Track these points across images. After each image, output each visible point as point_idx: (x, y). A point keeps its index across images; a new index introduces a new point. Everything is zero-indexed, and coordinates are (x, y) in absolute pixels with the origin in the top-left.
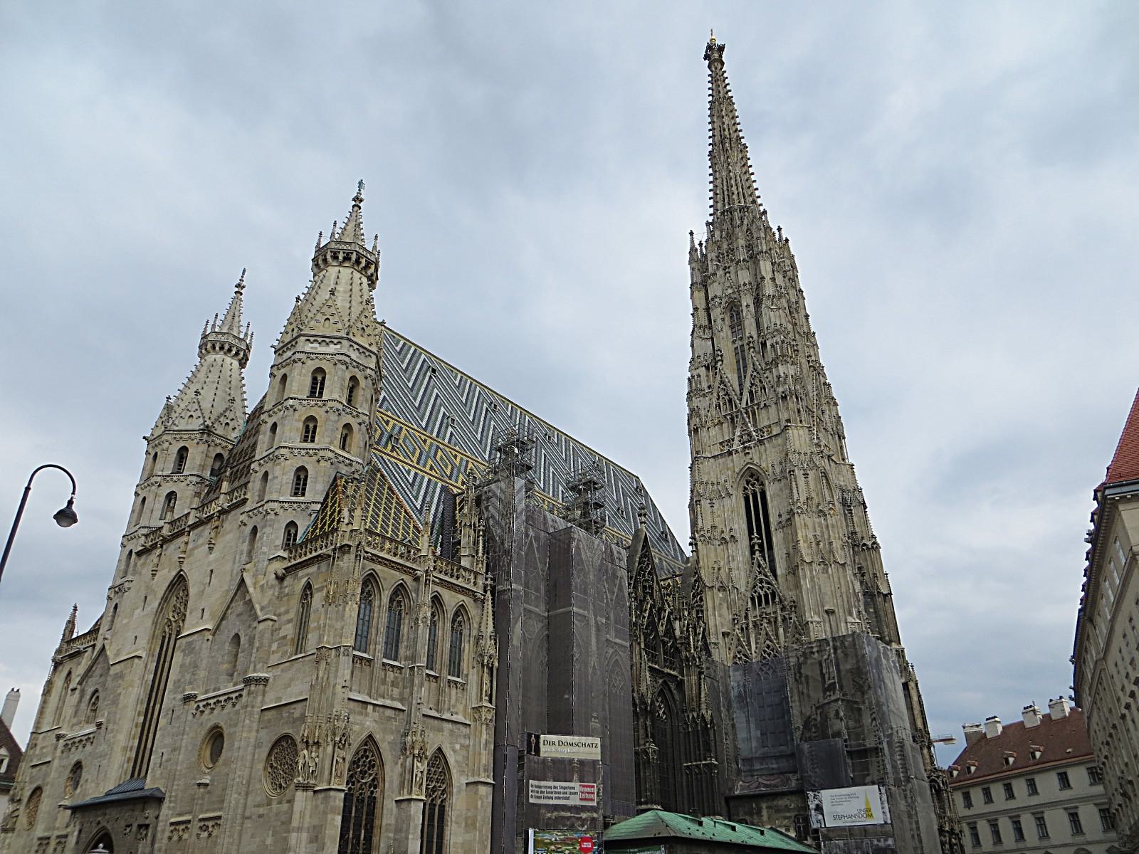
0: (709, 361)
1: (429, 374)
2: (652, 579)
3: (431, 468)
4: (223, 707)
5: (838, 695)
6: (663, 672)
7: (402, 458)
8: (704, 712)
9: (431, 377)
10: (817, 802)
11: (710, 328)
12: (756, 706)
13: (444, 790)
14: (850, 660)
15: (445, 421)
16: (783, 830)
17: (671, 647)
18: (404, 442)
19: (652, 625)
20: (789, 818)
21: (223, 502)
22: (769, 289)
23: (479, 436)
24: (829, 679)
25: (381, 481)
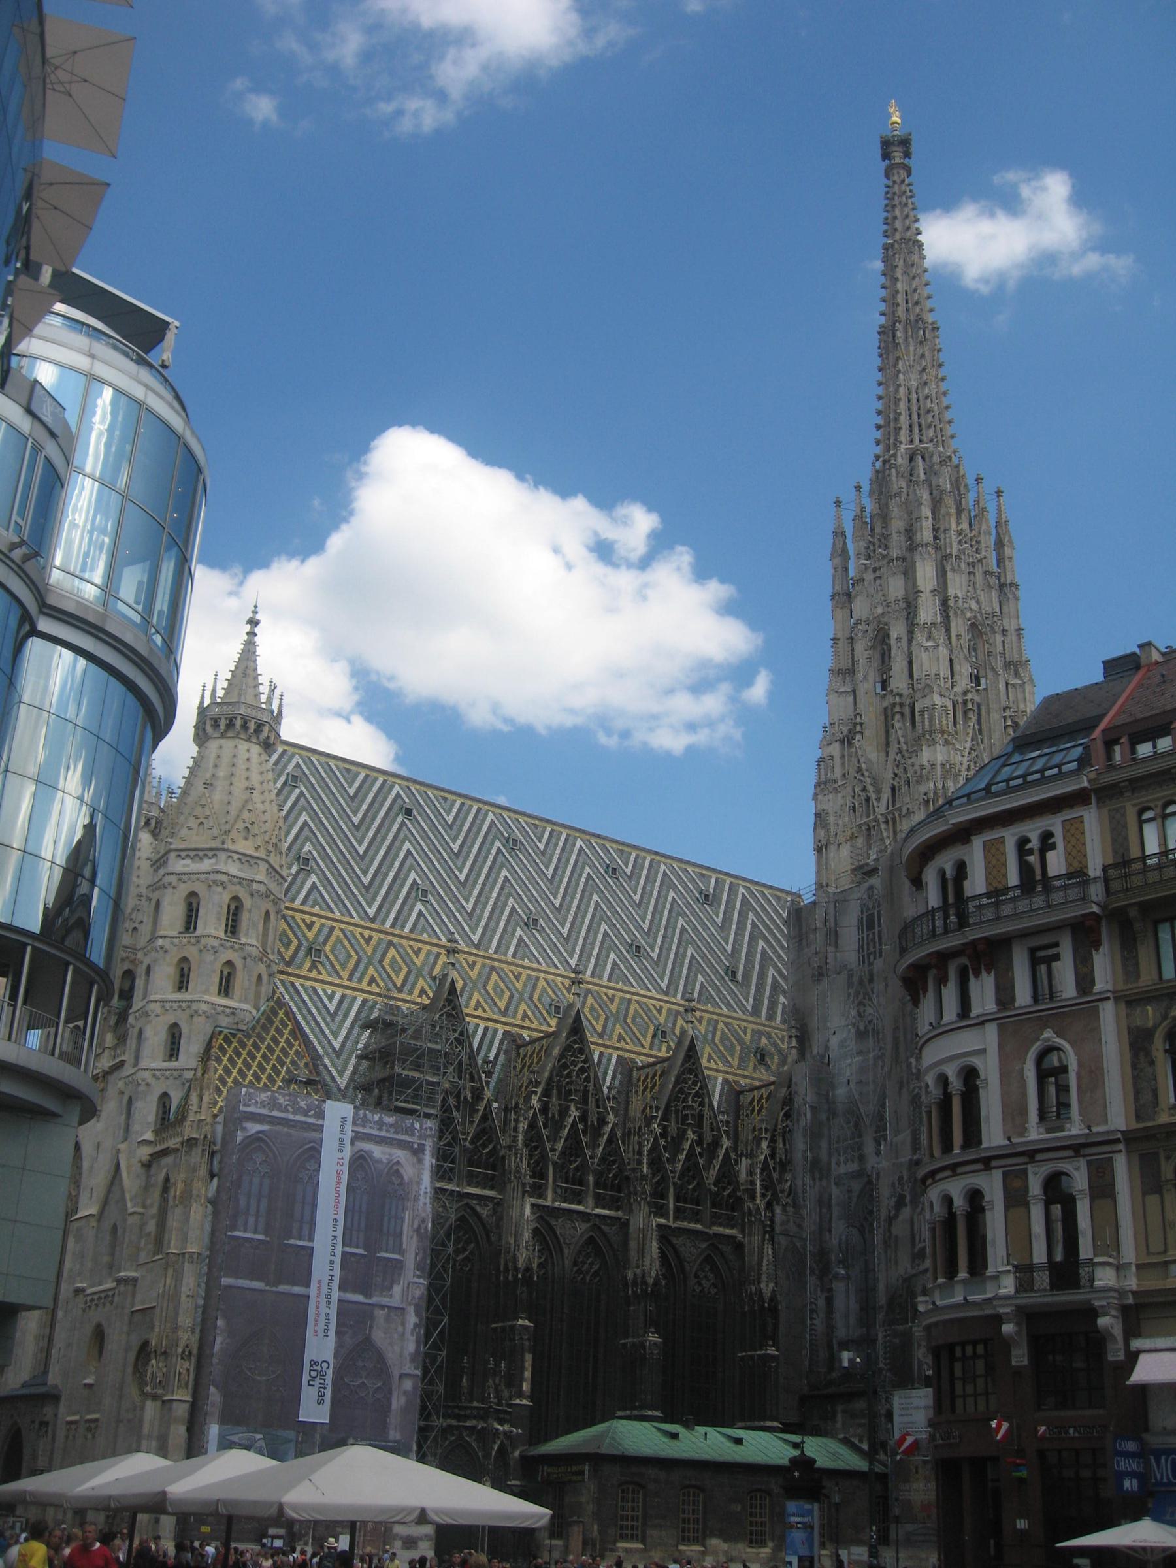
0: (845, 733)
1: (399, 819)
2: (702, 1104)
3: (372, 981)
4: (104, 1304)
5: (928, 1263)
6: (706, 1233)
7: (325, 977)
8: (763, 1286)
9: (403, 824)
11: (854, 672)
15: (413, 895)
16: (856, 1441)
17: (729, 1196)
19: (692, 1170)
21: (105, 1063)
23: (469, 907)
25: (282, 1021)
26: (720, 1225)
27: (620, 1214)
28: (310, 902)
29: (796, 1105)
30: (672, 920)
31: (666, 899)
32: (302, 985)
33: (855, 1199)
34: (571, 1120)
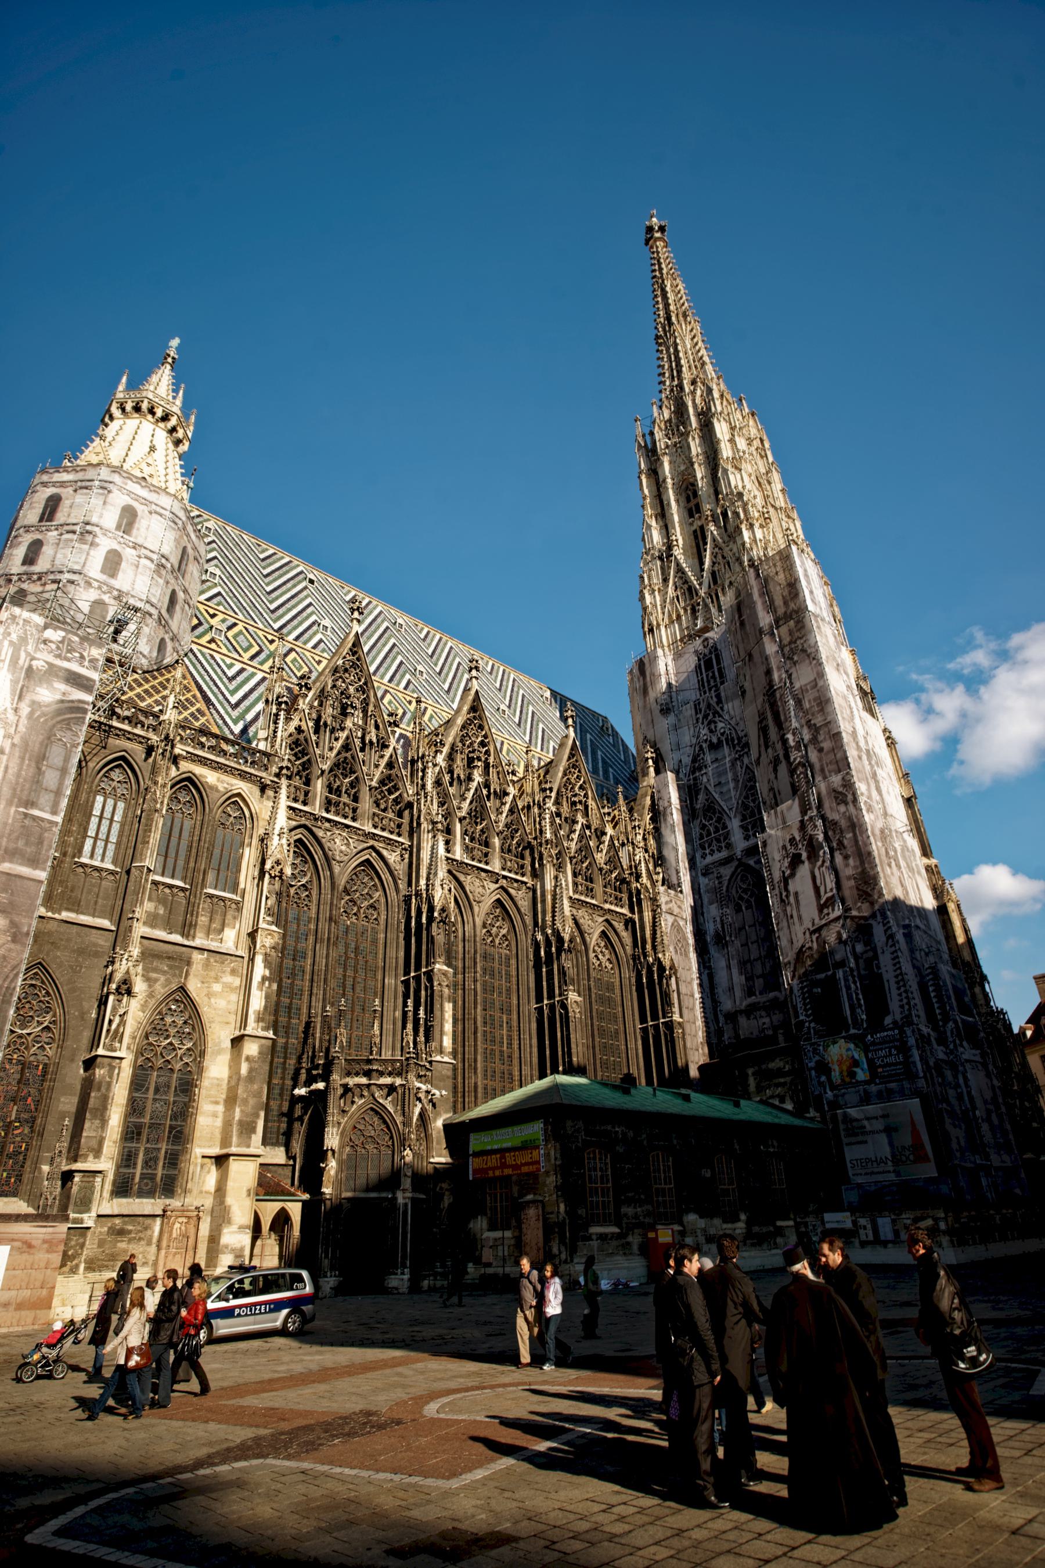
1: (304, 584)
2: (586, 796)
6: (602, 908)
7: (224, 651)
8: (660, 955)
9: (306, 588)
10: (817, 1058)
12: (738, 943)
13: (189, 1049)
14: (851, 861)
15: (315, 628)
16: (777, 1103)
18: (235, 637)
19: (584, 851)
20: (783, 1085)
22: (726, 451)
24: (826, 892)
26: (611, 903)
27: (524, 879)
28: (215, 601)
29: (661, 808)
30: (525, 705)
31: (518, 693)
32: (200, 651)
33: (726, 883)
34: (473, 785)
